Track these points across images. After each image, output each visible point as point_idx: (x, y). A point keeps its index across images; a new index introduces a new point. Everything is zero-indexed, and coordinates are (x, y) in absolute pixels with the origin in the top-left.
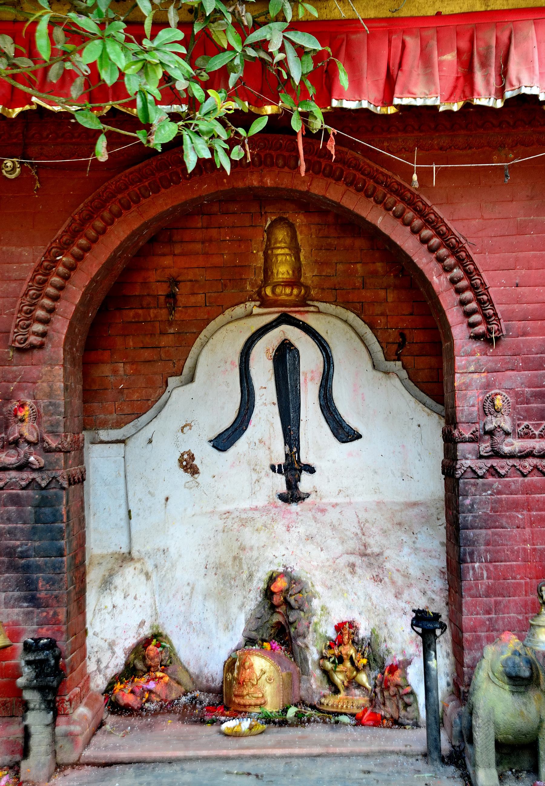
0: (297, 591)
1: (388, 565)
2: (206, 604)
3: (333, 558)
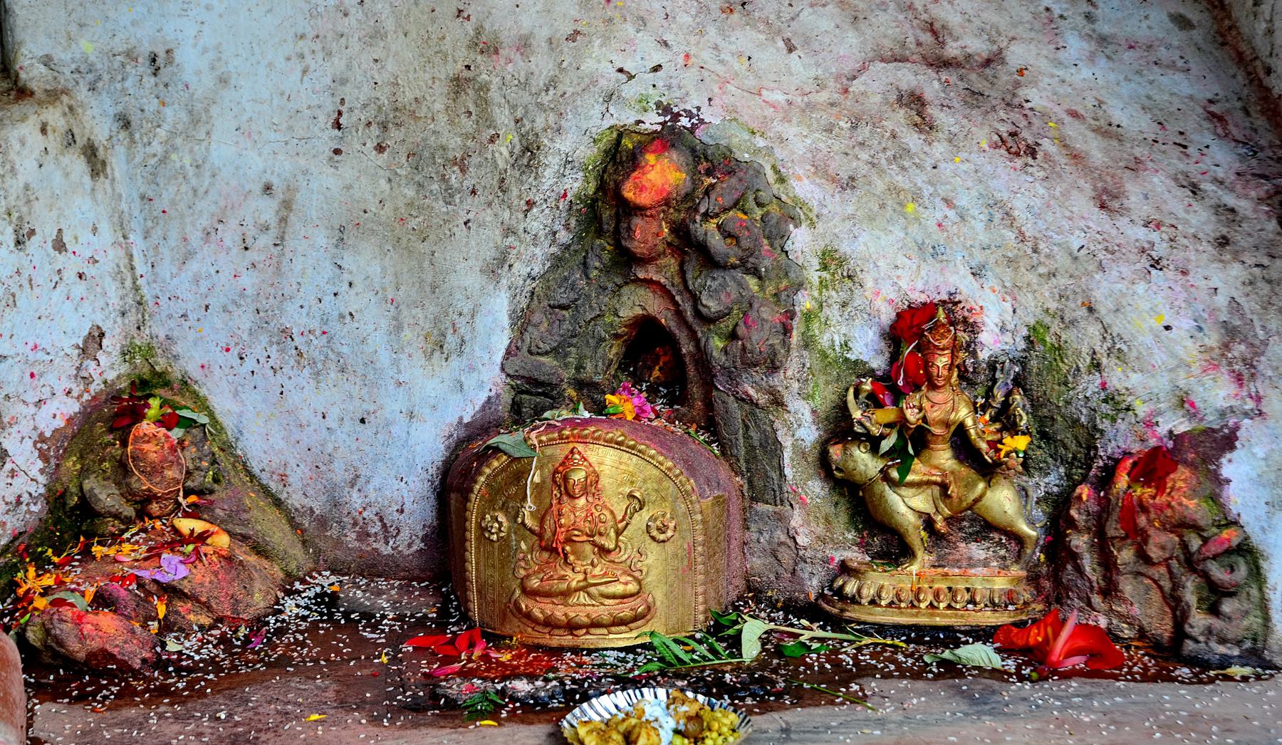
0: (727, 201)
1: (1036, 97)
2: (348, 261)
3: (838, 77)
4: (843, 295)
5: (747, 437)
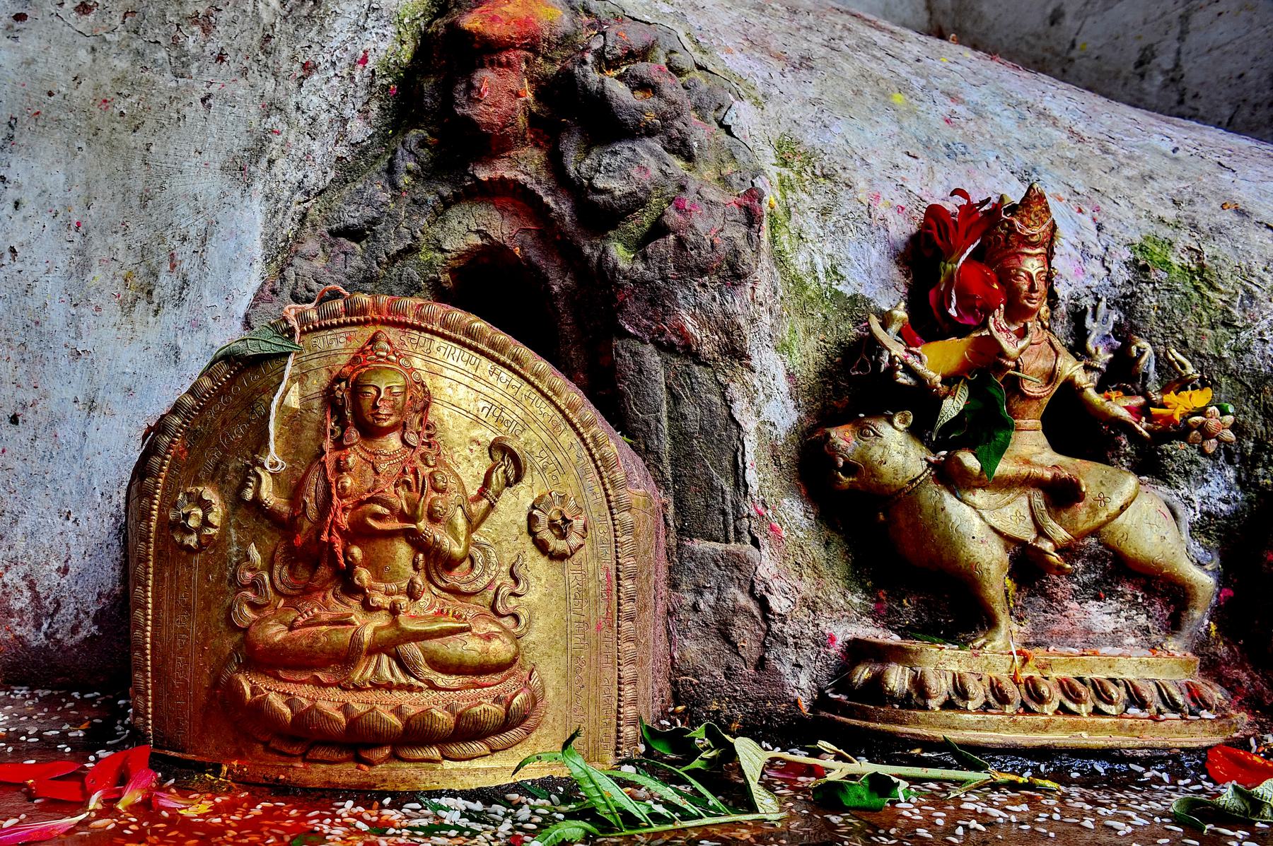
4: (821, 200)
5: (676, 417)
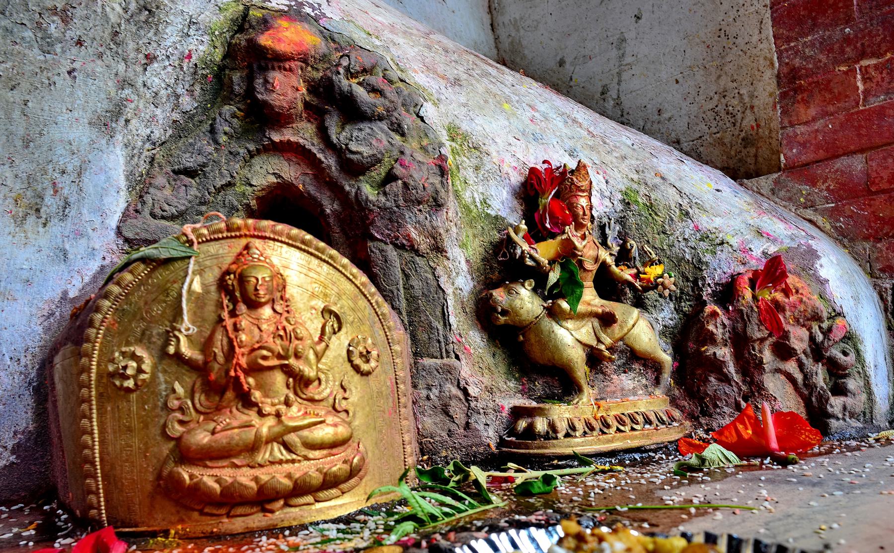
4: (475, 162)
5: (408, 288)
